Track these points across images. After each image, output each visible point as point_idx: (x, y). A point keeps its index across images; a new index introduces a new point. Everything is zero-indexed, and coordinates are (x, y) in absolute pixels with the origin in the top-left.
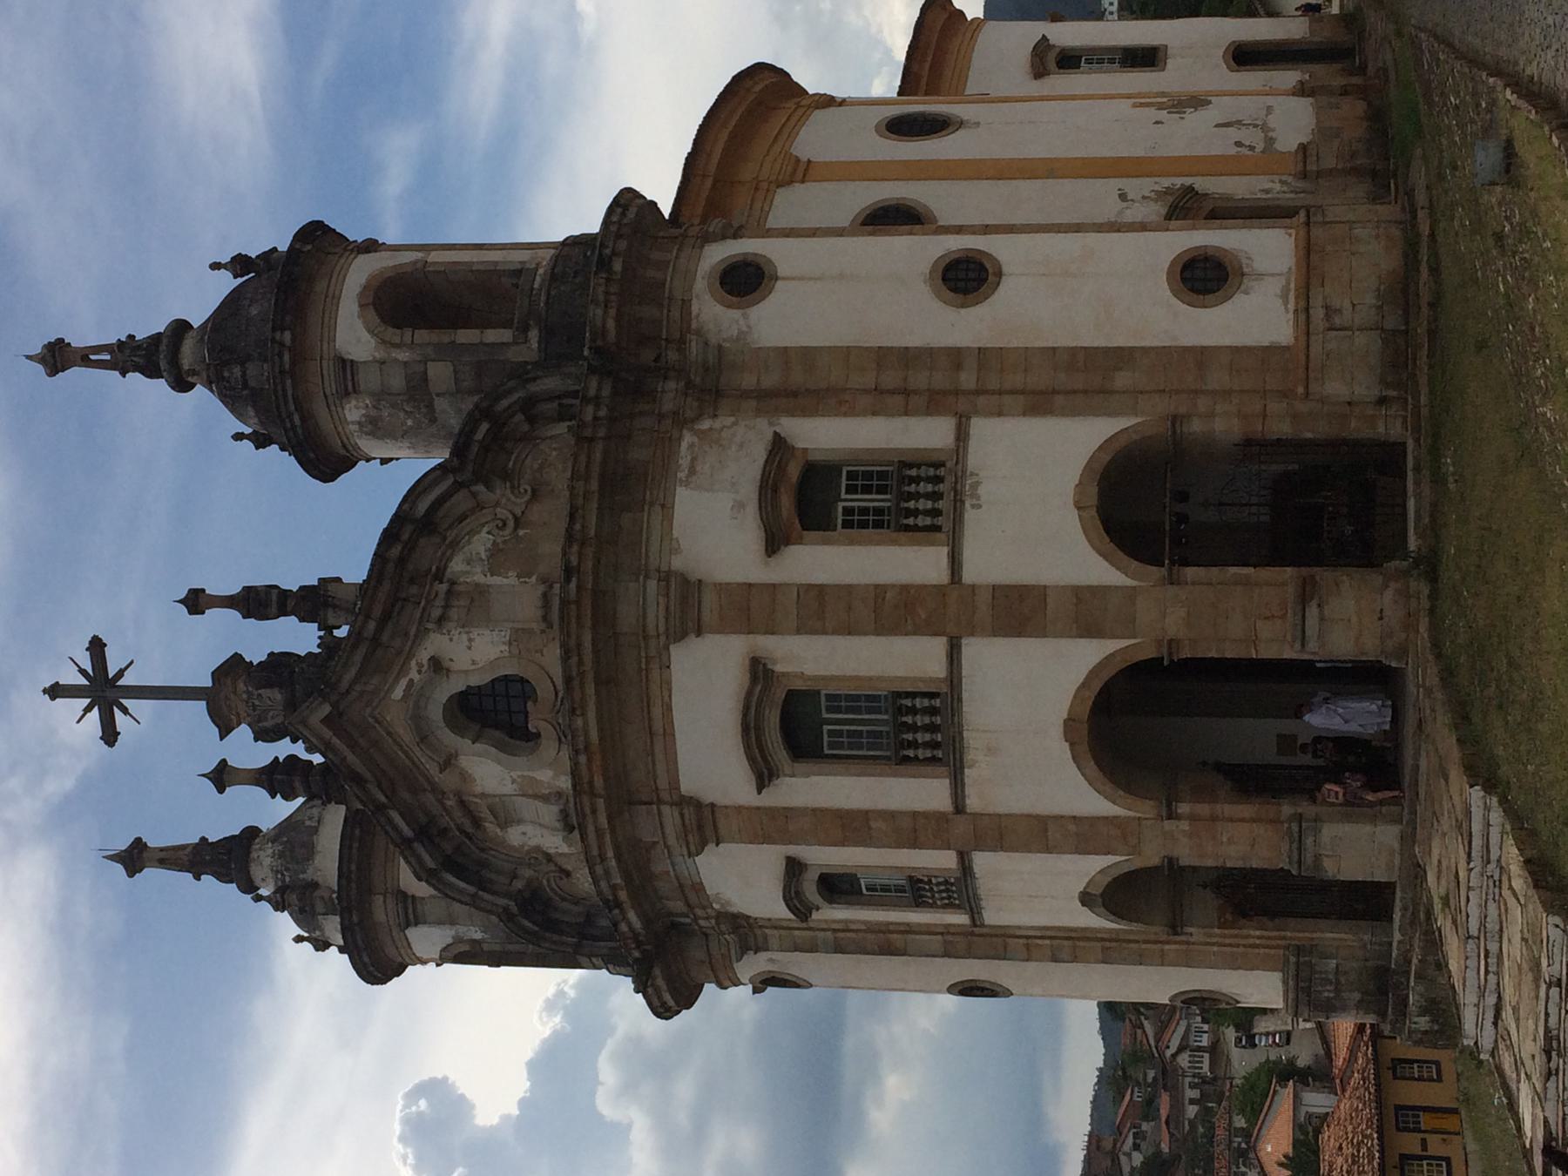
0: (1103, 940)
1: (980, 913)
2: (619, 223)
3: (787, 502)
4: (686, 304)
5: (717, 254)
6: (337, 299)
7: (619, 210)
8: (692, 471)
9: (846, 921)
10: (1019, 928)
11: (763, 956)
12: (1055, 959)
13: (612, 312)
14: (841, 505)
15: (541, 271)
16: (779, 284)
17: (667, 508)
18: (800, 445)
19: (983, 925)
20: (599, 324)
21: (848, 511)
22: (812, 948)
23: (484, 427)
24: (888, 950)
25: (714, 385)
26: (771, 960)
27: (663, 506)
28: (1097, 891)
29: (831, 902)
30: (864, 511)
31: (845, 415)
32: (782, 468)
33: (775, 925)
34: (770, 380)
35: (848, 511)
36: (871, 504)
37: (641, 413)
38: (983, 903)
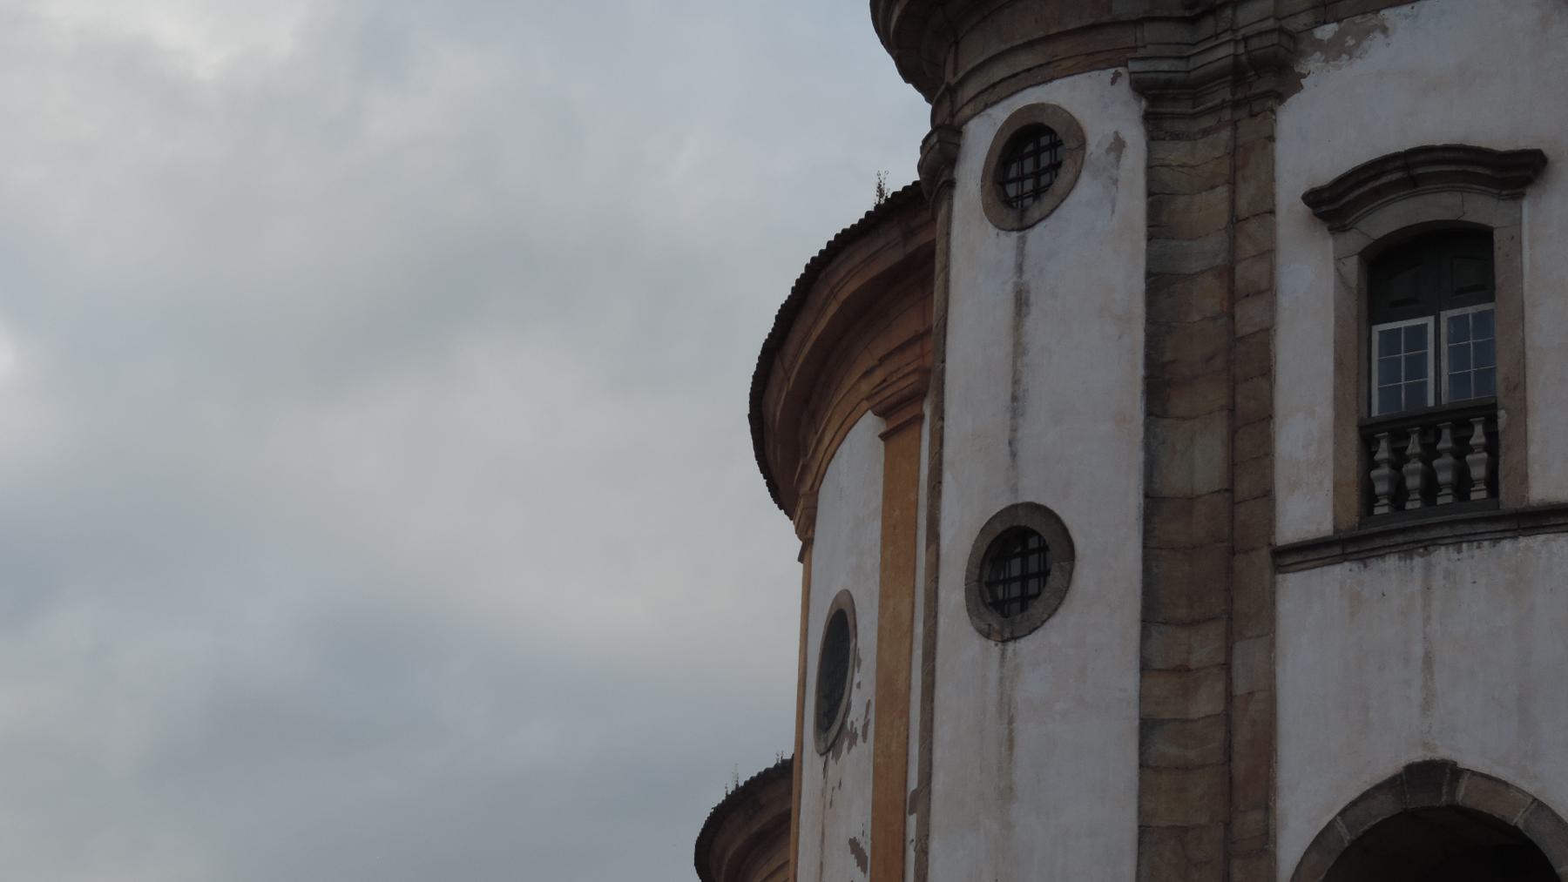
0: (1228, 825)
1: (1343, 558)
9: (1266, 291)
10: (1272, 645)
11: (1135, 136)
12: (1148, 727)
19: (1279, 568)
22: (1159, 225)
24: (1160, 386)
26: (1118, 145)
28: (1464, 795)
29: (1363, 255)
33: (1249, 157)
38: (1392, 562)
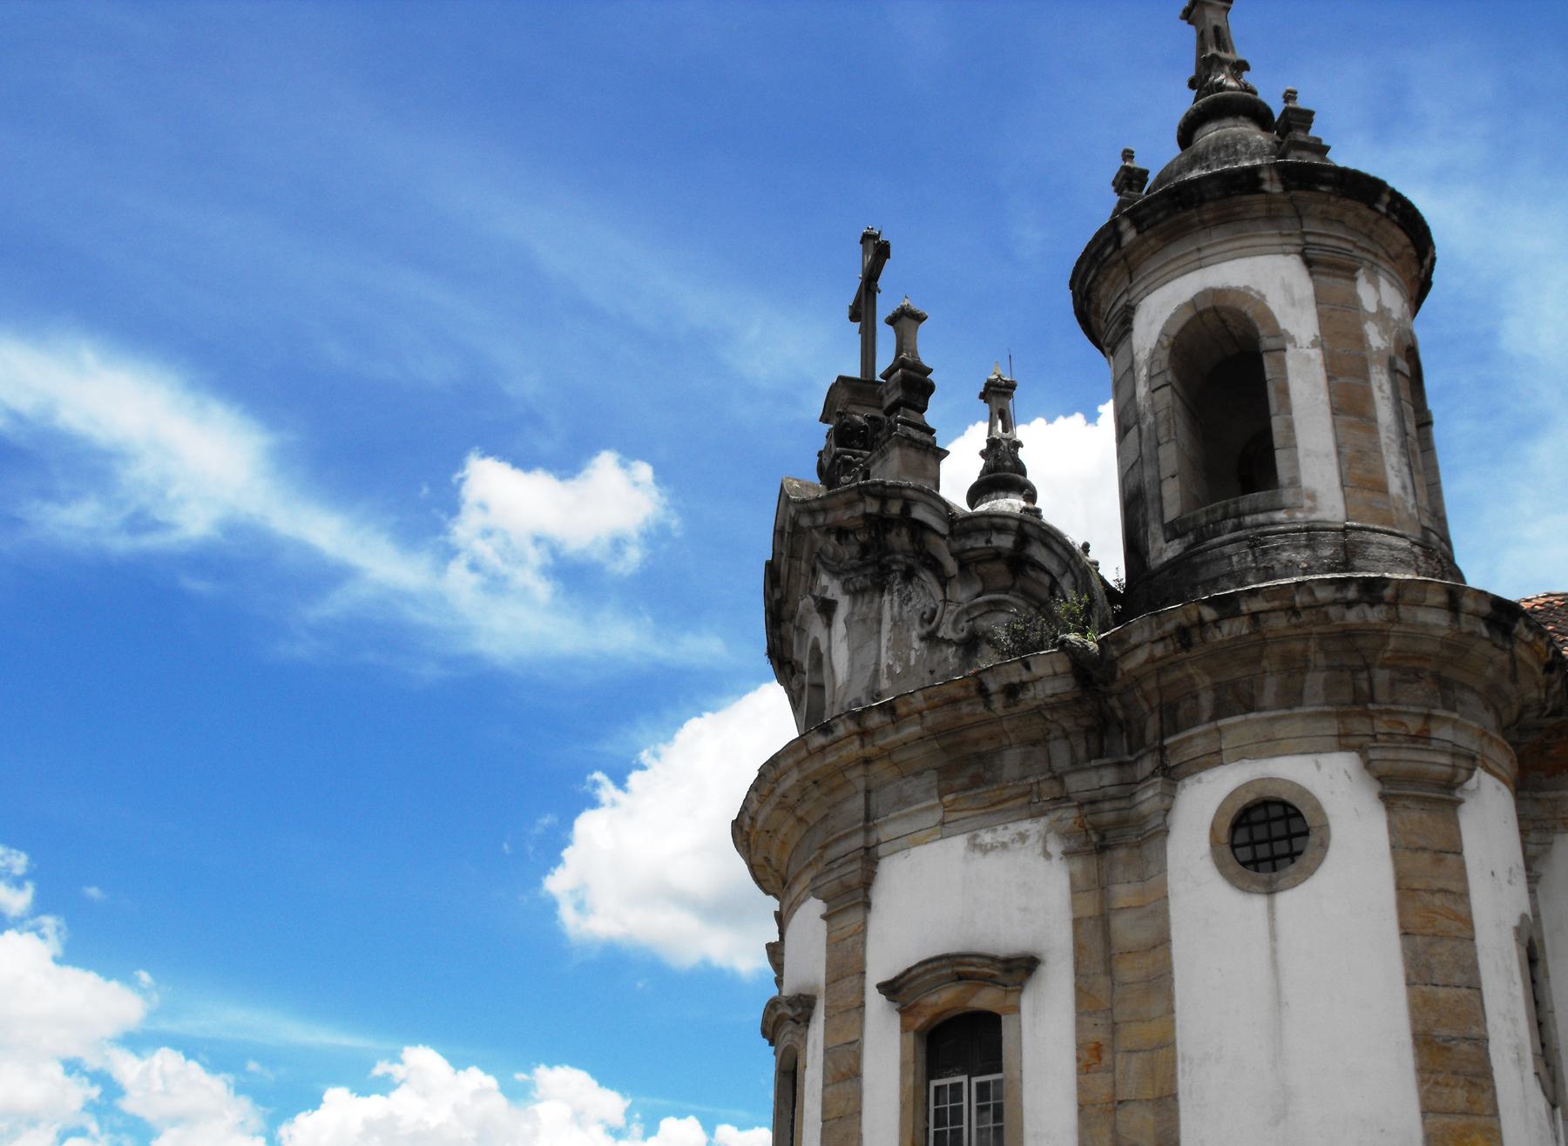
2: (1317, 606)
3: (944, 998)
4: (1215, 758)
5: (1332, 782)
6: (1200, 265)
7: (1352, 593)
8: (985, 850)
13: (1159, 650)
14: (963, 1079)
15: (1280, 516)
16: (1258, 903)
17: (944, 828)
18: (1027, 1002)
20: (1134, 640)
21: (957, 1088)
23: (1005, 542)
25: (1111, 843)
27: (943, 823)
30: (957, 1114)
31: (1078, 1059)
32: (989, 980)
34: (1127, 930)
35: (957, 1088)
36: (965, 1126)
37: (1072, 749)
